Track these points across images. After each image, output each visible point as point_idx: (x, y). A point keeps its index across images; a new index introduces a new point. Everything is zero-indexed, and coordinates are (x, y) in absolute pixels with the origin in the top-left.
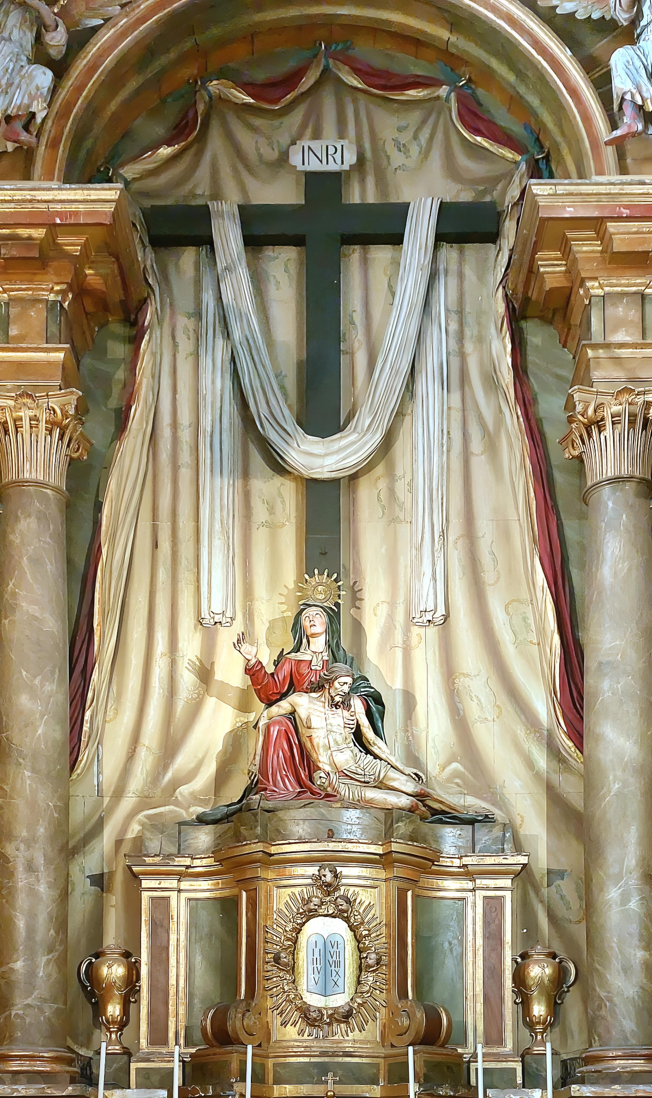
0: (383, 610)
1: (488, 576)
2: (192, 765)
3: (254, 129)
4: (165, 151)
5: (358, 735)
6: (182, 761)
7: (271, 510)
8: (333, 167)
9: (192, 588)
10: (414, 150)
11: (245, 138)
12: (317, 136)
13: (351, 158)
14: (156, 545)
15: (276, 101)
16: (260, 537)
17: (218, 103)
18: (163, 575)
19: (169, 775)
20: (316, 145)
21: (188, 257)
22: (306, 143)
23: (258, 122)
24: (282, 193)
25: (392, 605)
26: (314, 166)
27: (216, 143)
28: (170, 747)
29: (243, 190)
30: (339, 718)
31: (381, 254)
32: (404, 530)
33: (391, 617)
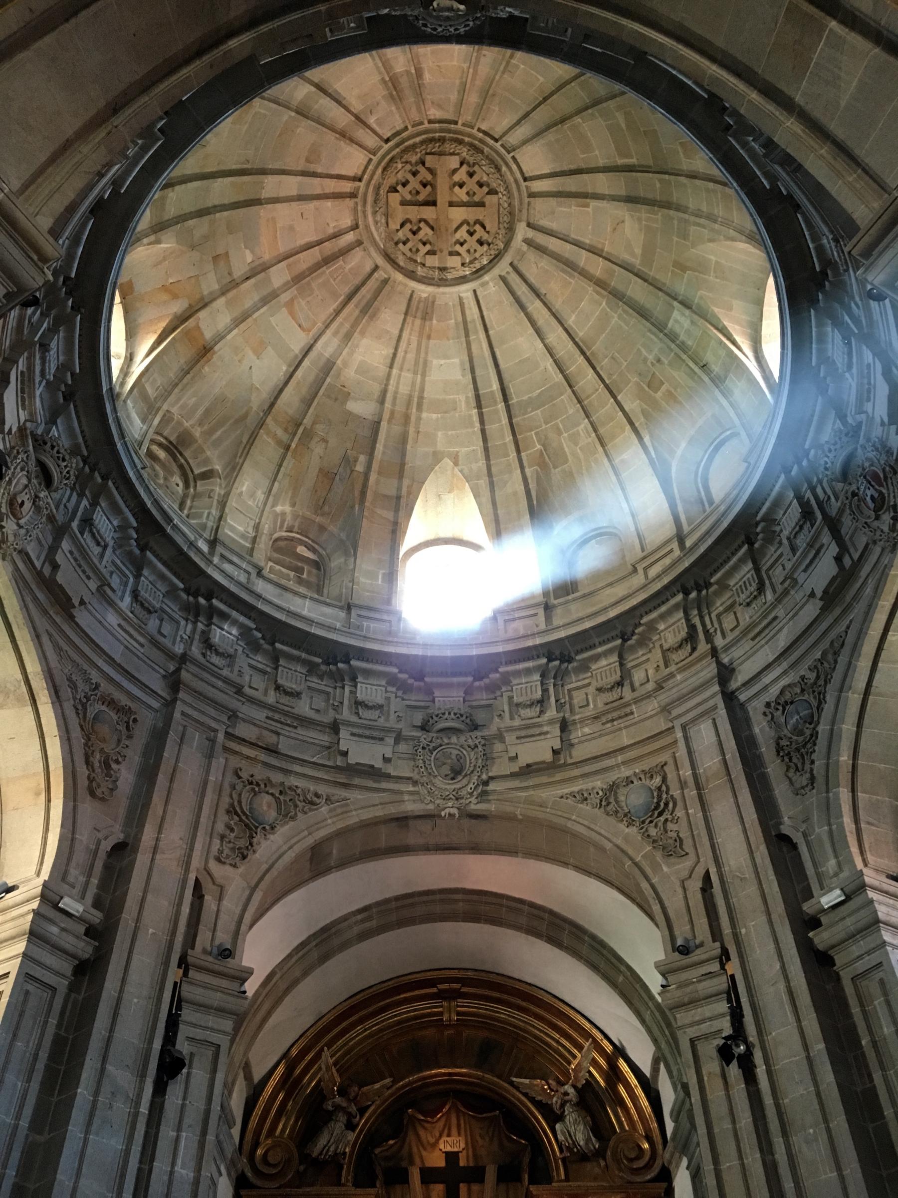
3: (425, 1129)
4: (391, 1142)
8: (456, 1150)
10: (487, 1139)
11: (422, 1133)
12: (449, 1135)
13: (463, 1145)
15: (432, 1117)
17: (412, 1118)
20: (448, 1139)
21: (398, 1188)
22: (445, 1138)
23: (426, 1125)
24: (437, 1160)
26: (449, 1149)
27: (411, 1136)
29: (421, 1157)
31: (475, 1187)
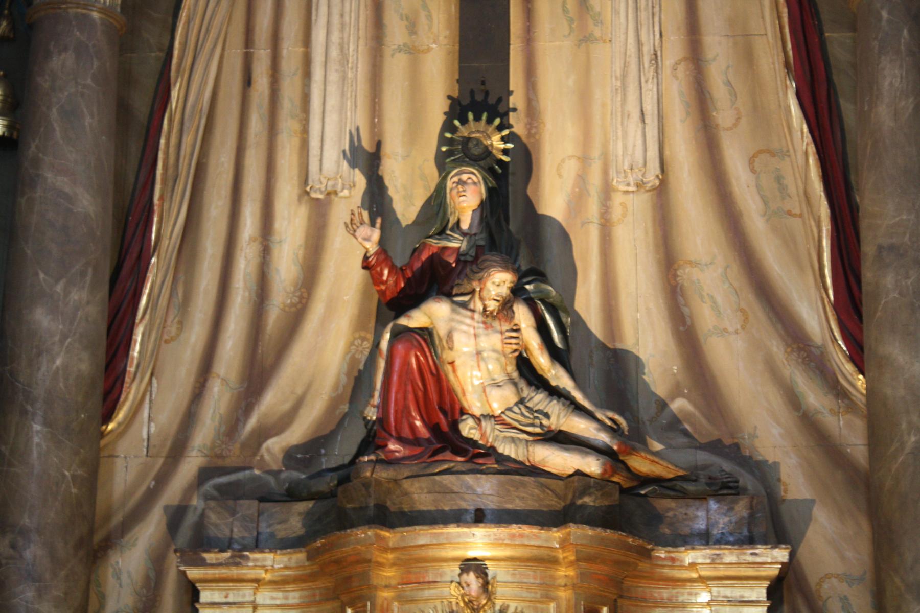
0: (571, 168)
1: (723, 116)
2: (287, 406)
5: (524, 365)
6: (272, 401)
7: (412, 28)
9: (296, 141)
14: (248, 81)
16: (396, 67)
18: (256, 125)
19: (252, 422)
25: (584, 160)
28: (257, 376)
30: (492, 341)
32: (600, 52)
33: (582, 178)
